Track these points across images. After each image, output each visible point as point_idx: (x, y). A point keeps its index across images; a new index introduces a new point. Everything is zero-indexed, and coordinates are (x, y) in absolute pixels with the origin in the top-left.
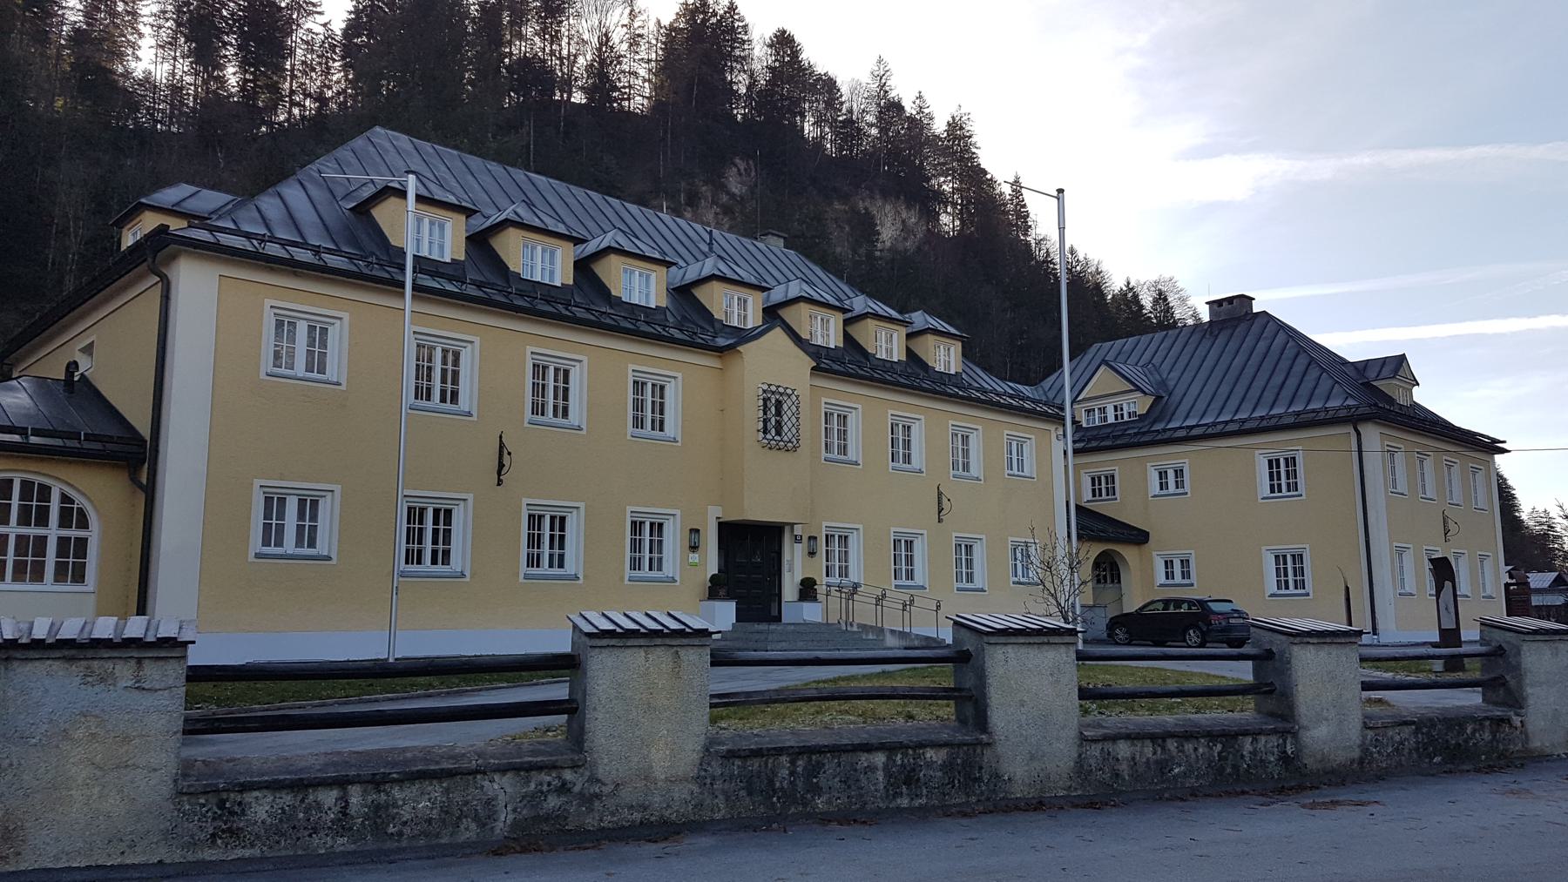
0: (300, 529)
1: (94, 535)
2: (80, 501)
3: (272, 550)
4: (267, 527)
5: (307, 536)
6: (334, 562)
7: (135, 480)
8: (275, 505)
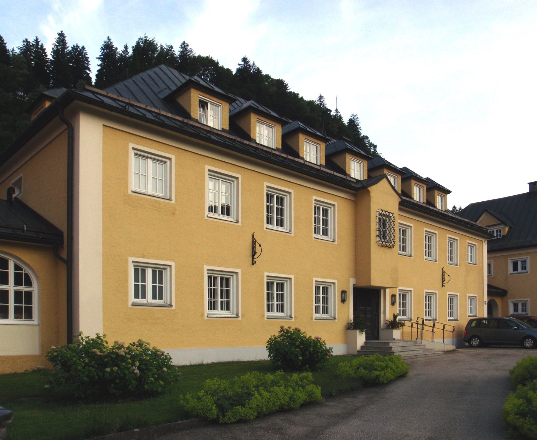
0: (154, 288)
1: (35, 289)
2: (26, 270)
3: (140, 301)
4: (136, 286)
5: (158, 293)
6: (174, 308)
7: (58, 257)
8: (140, 272)
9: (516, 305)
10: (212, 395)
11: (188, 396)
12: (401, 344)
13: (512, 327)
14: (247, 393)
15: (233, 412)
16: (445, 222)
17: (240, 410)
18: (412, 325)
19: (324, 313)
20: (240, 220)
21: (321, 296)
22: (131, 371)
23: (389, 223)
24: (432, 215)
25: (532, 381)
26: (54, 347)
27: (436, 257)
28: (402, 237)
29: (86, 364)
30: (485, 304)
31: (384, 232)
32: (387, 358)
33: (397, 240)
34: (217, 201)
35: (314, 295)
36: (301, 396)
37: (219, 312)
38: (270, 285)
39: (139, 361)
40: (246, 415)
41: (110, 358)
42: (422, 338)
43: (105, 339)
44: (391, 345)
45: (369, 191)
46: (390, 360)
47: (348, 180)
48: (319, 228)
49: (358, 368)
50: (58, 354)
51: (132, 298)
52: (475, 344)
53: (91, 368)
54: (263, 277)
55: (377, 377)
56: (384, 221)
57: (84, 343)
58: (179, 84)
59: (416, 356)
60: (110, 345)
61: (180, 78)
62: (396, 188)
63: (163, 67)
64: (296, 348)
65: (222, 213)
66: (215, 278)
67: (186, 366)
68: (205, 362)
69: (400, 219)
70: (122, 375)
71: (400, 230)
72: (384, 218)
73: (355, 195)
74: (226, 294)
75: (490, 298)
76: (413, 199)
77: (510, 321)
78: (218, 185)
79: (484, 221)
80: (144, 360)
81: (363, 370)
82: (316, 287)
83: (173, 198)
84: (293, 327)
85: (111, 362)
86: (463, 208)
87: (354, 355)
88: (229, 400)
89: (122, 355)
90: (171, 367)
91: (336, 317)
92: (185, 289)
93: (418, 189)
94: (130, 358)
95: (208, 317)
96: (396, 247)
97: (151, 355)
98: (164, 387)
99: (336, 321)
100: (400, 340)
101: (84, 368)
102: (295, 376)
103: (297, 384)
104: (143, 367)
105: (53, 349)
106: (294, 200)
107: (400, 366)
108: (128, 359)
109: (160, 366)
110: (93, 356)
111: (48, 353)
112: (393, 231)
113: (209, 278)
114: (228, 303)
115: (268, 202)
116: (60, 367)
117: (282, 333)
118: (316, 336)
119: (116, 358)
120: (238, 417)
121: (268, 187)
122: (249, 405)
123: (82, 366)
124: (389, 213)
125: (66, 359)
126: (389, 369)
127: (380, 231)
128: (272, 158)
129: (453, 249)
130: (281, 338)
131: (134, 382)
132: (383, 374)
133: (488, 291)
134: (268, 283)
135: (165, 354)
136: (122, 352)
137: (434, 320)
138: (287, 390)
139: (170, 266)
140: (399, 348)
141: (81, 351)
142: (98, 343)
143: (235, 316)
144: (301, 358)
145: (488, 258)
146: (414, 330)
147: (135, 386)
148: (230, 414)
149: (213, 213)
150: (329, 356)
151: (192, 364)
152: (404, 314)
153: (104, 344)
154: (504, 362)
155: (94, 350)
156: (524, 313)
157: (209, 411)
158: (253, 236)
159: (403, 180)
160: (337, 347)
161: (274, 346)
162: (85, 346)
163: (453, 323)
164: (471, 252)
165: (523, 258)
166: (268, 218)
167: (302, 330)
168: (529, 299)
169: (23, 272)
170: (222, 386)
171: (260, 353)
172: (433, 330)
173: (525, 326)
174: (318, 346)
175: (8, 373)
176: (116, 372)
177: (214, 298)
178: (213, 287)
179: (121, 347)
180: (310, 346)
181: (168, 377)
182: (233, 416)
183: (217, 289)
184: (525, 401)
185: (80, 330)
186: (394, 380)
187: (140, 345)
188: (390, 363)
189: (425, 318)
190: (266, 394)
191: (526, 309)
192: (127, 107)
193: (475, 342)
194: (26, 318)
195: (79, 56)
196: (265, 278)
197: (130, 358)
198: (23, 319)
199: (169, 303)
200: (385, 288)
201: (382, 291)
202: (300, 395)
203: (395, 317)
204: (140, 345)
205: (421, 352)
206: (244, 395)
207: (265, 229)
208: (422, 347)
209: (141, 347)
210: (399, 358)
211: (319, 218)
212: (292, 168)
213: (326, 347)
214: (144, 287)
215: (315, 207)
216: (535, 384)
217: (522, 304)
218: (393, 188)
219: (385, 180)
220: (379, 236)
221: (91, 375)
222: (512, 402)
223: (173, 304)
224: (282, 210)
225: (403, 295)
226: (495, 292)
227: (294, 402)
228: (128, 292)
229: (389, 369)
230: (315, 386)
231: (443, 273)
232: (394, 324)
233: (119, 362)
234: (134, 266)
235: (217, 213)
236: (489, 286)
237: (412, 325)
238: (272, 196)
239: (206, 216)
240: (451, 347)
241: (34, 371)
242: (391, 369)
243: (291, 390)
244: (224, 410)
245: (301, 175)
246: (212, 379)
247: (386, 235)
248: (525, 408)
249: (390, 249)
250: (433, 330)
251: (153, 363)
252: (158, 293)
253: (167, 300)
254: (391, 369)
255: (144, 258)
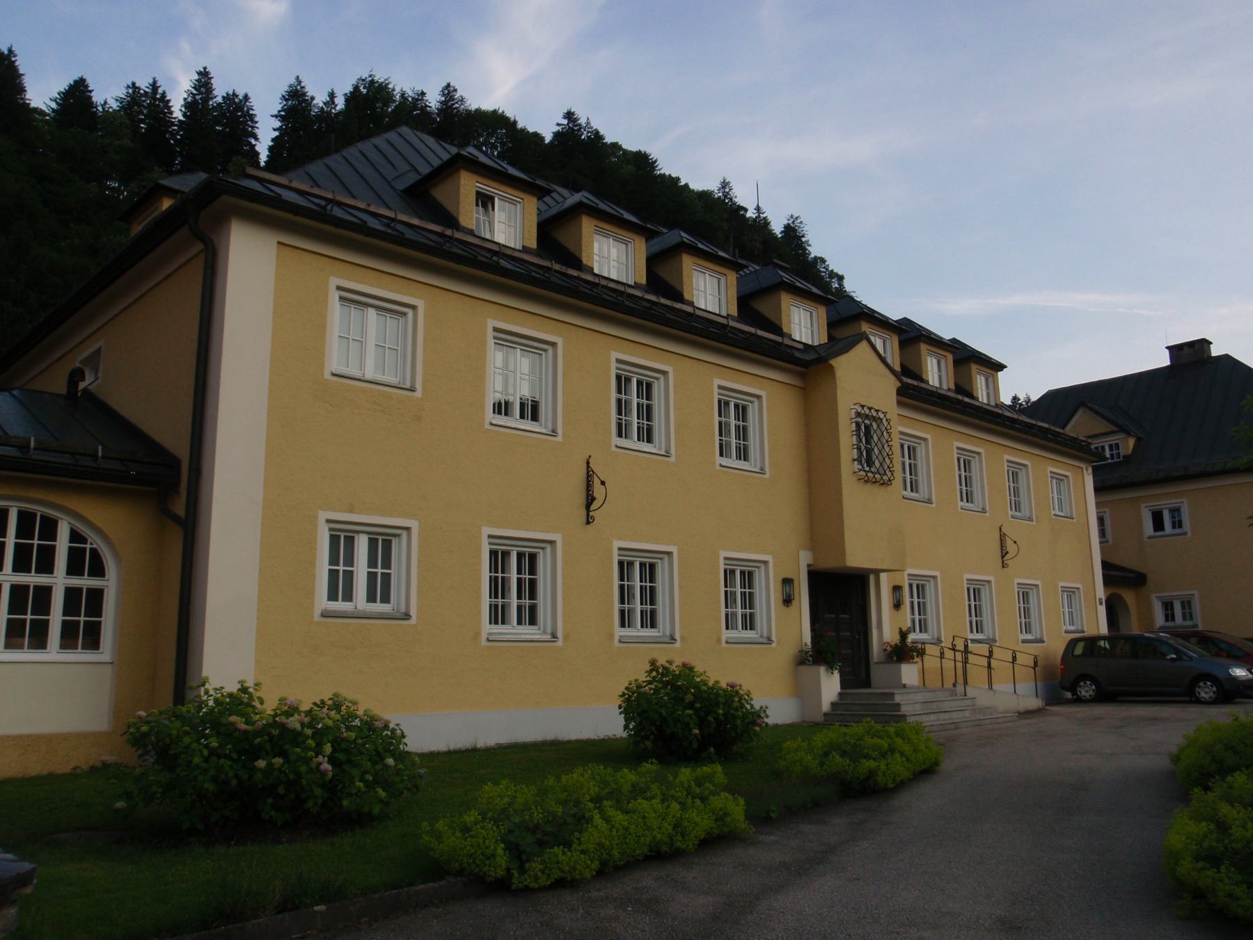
0: (372, 577)
1: (110, 585)
2: (94, 541)
3: (340, 605)
4: (333, 575)
5: (380, 588)
6: (413, 621)
8: (342, 543)
9: (1168, 606)
10: (496, 822)
11: (440, 825)
12: (920, 697)
13: (1164, 655)
14: (574, 815)
15: (544, 862)
16: (998, 428)
17: (561, 857)
18: (942, 654)
19: (745, 627)
20: (560, 431)
21: (739, 590)
22: (314, 765)
23: (879, 432)
24: (970, 415)
25: (1223, 780)
26: (142, 713)
27: (984, 504)
28: (907, 462)
29: (213, 752)
30: (1101, 603)
31: (869, 452)
32: (892, 730)
33: (897, 468)
34: (511, 391)
35: (723, 589)
36: (701, 822)
37: (513, 630)
38: (624, 568)
39: (333, 742)
40: (574, 868)
41: (266, 738)
42: (966, 683)
43: (258, 694)
44: (898, 699)
45: (832, 367)
46: (897, 734)
47: (787, 346)
48: (729, 444)
49: (826, 754)
50: (151, 729)
51: (321, 601)
52: (1087, 695)
53: (222, 761)
54: (610, 551)
55: (872, 774)
56: (867, 428)
57: (211, 703)
58: (436, 163)
59: (956, 725)
60: (269, 707)
61: (440, 152)
62: (889, 361)
63: (405, 130)
64: (685, 708)
65: (522, 416)
66: (506, 554)
67: (439, 753)
68: (480, 745)
69: (903, 425)
70: (292, 776)
71: (902, 446)
72: (867, 422)
73: (802, 376)
74: (529, 589)
75: (1111, 591)
76: (927, 382)
77: (1160, 640)
78: (513, 359)
79: (1080, 425)
80: (343, 739)
81: (838, 759)
82: (725, 571)
83: (419, 386)
84: (678, 662)
85: (268, 746)
86: (1034, 398)
87: (817, 724)
88: (534, 833)
89: (294, 730)
90: (403, 756)
91: (774, 638)
92: (441, 582)
93: (935, 361)
94: (313, 737)
95: (488, 640)
96: (898, 482)
97: (359, 729)
98: (386, 804)
99: (774, 645)
100: (919, 687)
101: (206, 760)
102: (686, 774)
103: (689, 792)
104: (341, 756)
105: (140, 717)
106: (675, 387)
107: (922, 747)
108: (307, 737)
109: (378, 754)
110: (227, 733)
111: (129, 727)
112: (887, 449)
113: (493, 553)
114: (533, 609)
115: (619, 392)
116: (152, 760)
117: (654, 674)
118: (731, 679)
119: (280, 737)
120: (556, 874)
121: (618, 361)
122: (580, 844)
123: (202, 756)
124: (877, 411)
125: (168, 741)
126: (897, 755)
127: (859, 449)
128: (627, 303)
129: (1020, 486)
130: (652, 686)
131: (318, 791)
132: (883, 767)
133: (1104, 575)
134: (621, 564)
135: (392, 726)
136: (294, 722)
137: (991, 642)
138: (668, 807)
139: (408, 529)
140: (918, 707)
141: (203, 721)
142: (241, 703)
143: (548, 637)
144: (697, 731)
145: (1098, 505)
146: (948, 664)
147: (320, 802)
148: (535, 866)
149: (503, 417)
150: (760, 725)
151: (452, 748)
152: (923, 627)
153: (256, 704)
154: (1155, 736)
155: (233, 718)
156: (1188, 623)
157: (488, 859)
158: (588, 463)
159: (903, 344)
160: (778, 708)
161: (635, 705)
162: (212, 710)
163: (1034, 649)
164: (1059, 493)
165: (1174, 502)
166: (619, 426)
167: (699, 668)
168: (1195, 592)
169: (88, 546)
170: (520, 800)
171: (608, 723)
172: (989, 664)
173: (1193, 651)
174: (736, 704)
175: (33, 774)
176: (280, 771)
177: (503, 597)
178: (500, 575)
179: (292, 710)
180: (717, 704)
181: (397, 779)
182: (543, 872)
183: (509, 578)
184: (1212, 826)
185: (204, 674)
186: (910, 780)
187: (337, 706)
188: (899, 741)
189: (971, 636)
190: (619, 817)
191: (1191, 614)
192: (329, 207)
193: (1086, 690)
194: (86, 647)
195: (237, 114)
196: (616, 552)
197: (313, 737)
198: (79, 650)
199: (403, 610)
200: (877, 572)
201: (872, 578)
202: (698, 820)
203: (903, 635)
204: (337, 706)
205: (967, 714)
206: (569, 820)
207: (614, 449)
208: (968, 702)
209: (339, 711)
210: (917, 729)
211: (727, 424)
212: (668, 323)
213: (752, 706)
214: (349, 576)
215: (720, 402)
216: (1230, 787)
217: (1183, 603)
218: (883, 360)
219: (864, 344)
220: (859, 460)
221: (223, 776)
222: (1184, 831)
223: (413, 612)
224: (649, 408)
225: (918, 586)
226: (1121, 577)
227: (683, 836)
228: (313, 588)
229: (897, 755)
230: (730, 797)
231: (1002, 537)
232: (902, 652)
233: (287, 747)
234: (331, 529)
235: (512, 416)
236: (1106, 565)
237: (942, 654)
238: (628, 380)
239: (487, 422)
240: (1035, 703)
241: (93, 769)
242: (902, 754)
243: (675, 806)
244: (524, 857)
245: (687, 335)
246: (497, 783)
247: (874, 457)
248: (1215, 844)
249: (884, 488)
250: (989, 664)
251: (363, 746)
252: (380, 588)
253: (398, 604)
254: (902, 754)
255: (351, 511)
